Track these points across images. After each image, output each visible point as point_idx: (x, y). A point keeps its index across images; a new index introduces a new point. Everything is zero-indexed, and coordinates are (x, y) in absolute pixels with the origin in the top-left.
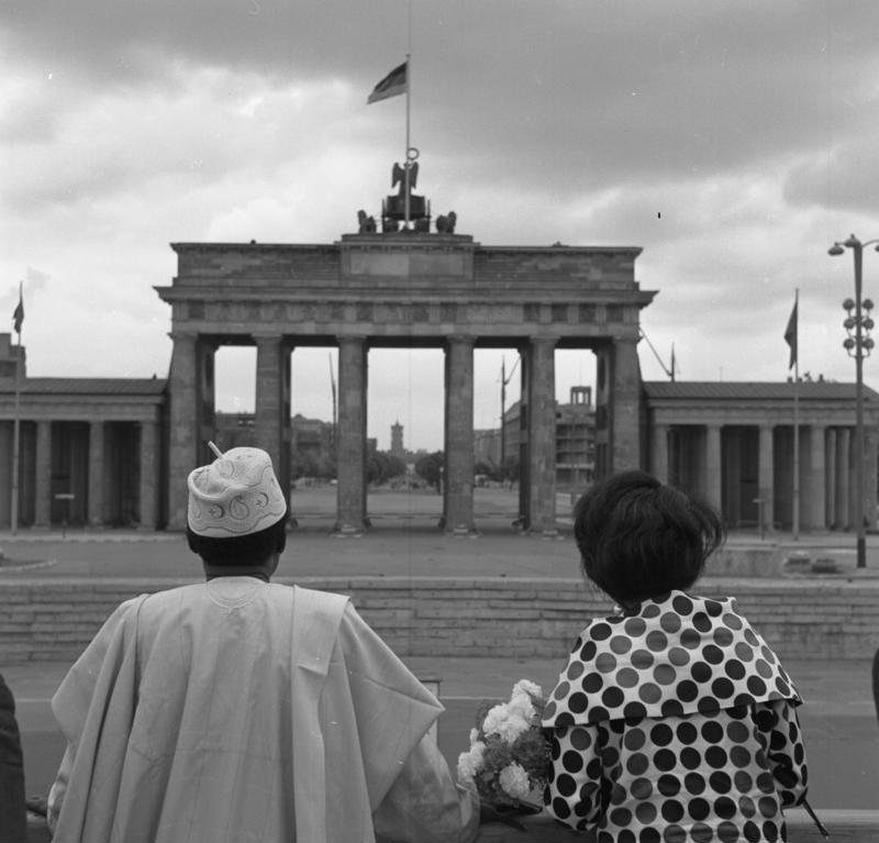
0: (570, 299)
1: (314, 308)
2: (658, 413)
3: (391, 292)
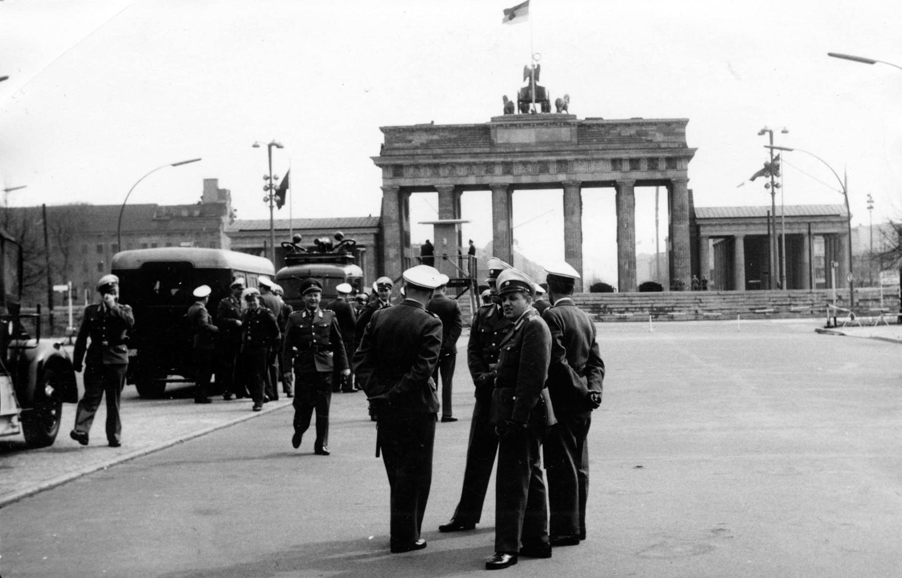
0: (641, 154)
1: (474, 167)
2: (702, 229)
3: (524, 154)
